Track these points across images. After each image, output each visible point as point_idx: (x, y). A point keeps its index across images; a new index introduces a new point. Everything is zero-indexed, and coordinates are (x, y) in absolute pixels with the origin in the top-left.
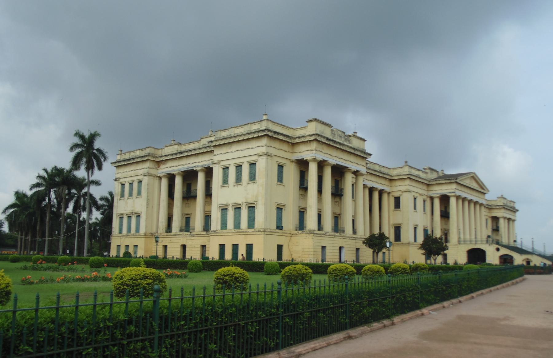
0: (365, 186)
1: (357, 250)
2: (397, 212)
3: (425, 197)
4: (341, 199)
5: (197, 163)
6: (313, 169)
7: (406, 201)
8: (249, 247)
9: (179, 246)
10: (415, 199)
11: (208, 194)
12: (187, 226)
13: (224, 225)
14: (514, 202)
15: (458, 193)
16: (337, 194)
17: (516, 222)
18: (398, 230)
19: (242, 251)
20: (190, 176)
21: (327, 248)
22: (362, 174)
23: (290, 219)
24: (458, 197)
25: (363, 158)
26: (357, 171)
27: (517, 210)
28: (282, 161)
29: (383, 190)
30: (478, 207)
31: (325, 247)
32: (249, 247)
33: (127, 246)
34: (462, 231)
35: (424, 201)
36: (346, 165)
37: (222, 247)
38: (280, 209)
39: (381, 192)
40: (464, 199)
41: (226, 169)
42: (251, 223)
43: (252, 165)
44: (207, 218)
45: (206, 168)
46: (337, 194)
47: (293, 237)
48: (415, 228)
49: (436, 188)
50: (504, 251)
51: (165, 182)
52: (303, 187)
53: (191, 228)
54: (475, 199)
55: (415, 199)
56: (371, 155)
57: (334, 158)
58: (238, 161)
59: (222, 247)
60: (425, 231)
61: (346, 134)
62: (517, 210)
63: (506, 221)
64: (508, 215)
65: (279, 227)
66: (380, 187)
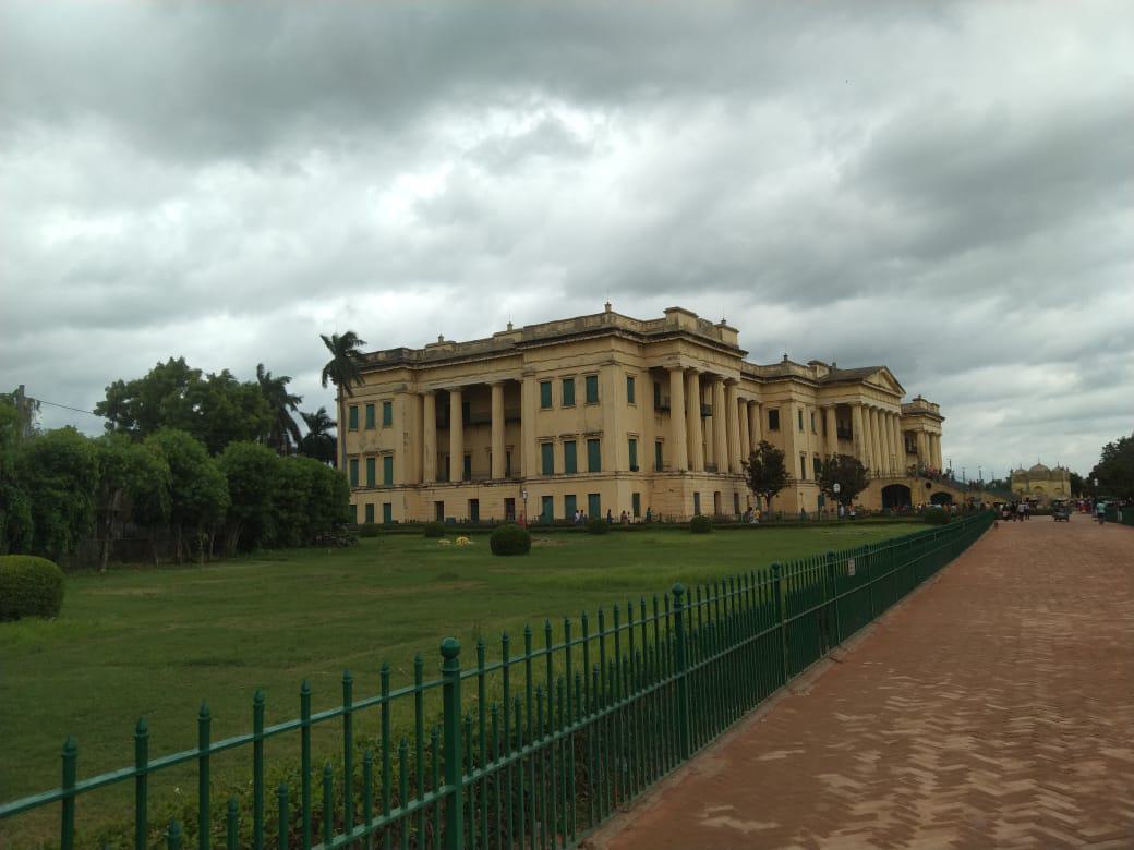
2: (775, 434)
3: (813, 408)
5: (491, 375)
7: (790, 416)
8: (594, 498)
9: (466, 502)
10: (800, 413)
11: (513, 420)
13: (548, 469)
14: (938, 406)
15: (864, 400)
16: (706, 412)
17: (941, 438)
19: (582, 504)
20: (475, 395)
21: (701, 495)
22: (736, 383)
23: (645, 458)
24: (864, 407)
25: (737, 359)
28: (632, 371)
30: (891, 418)
32: (594, 498)
36: (717, 372)
37: (547, 500)
38: (632, 443)
39: (750, 405)
40: (872, 409)
41: (546, 386)
42: (595, 464)
43: (592, 380)
44: (510, 453)
48: (803, 459)
49: (830, 393)
50: (938, 488)
51: (429, 404)
52: (662, 409)
54: (887, 407)
55: (800, 413)
56: (747, 353)
59: (547, 500)
60: (816, 461)
62: (943, 419)
63: (928, 437)
64: (929, 426)
65: (634, 468)
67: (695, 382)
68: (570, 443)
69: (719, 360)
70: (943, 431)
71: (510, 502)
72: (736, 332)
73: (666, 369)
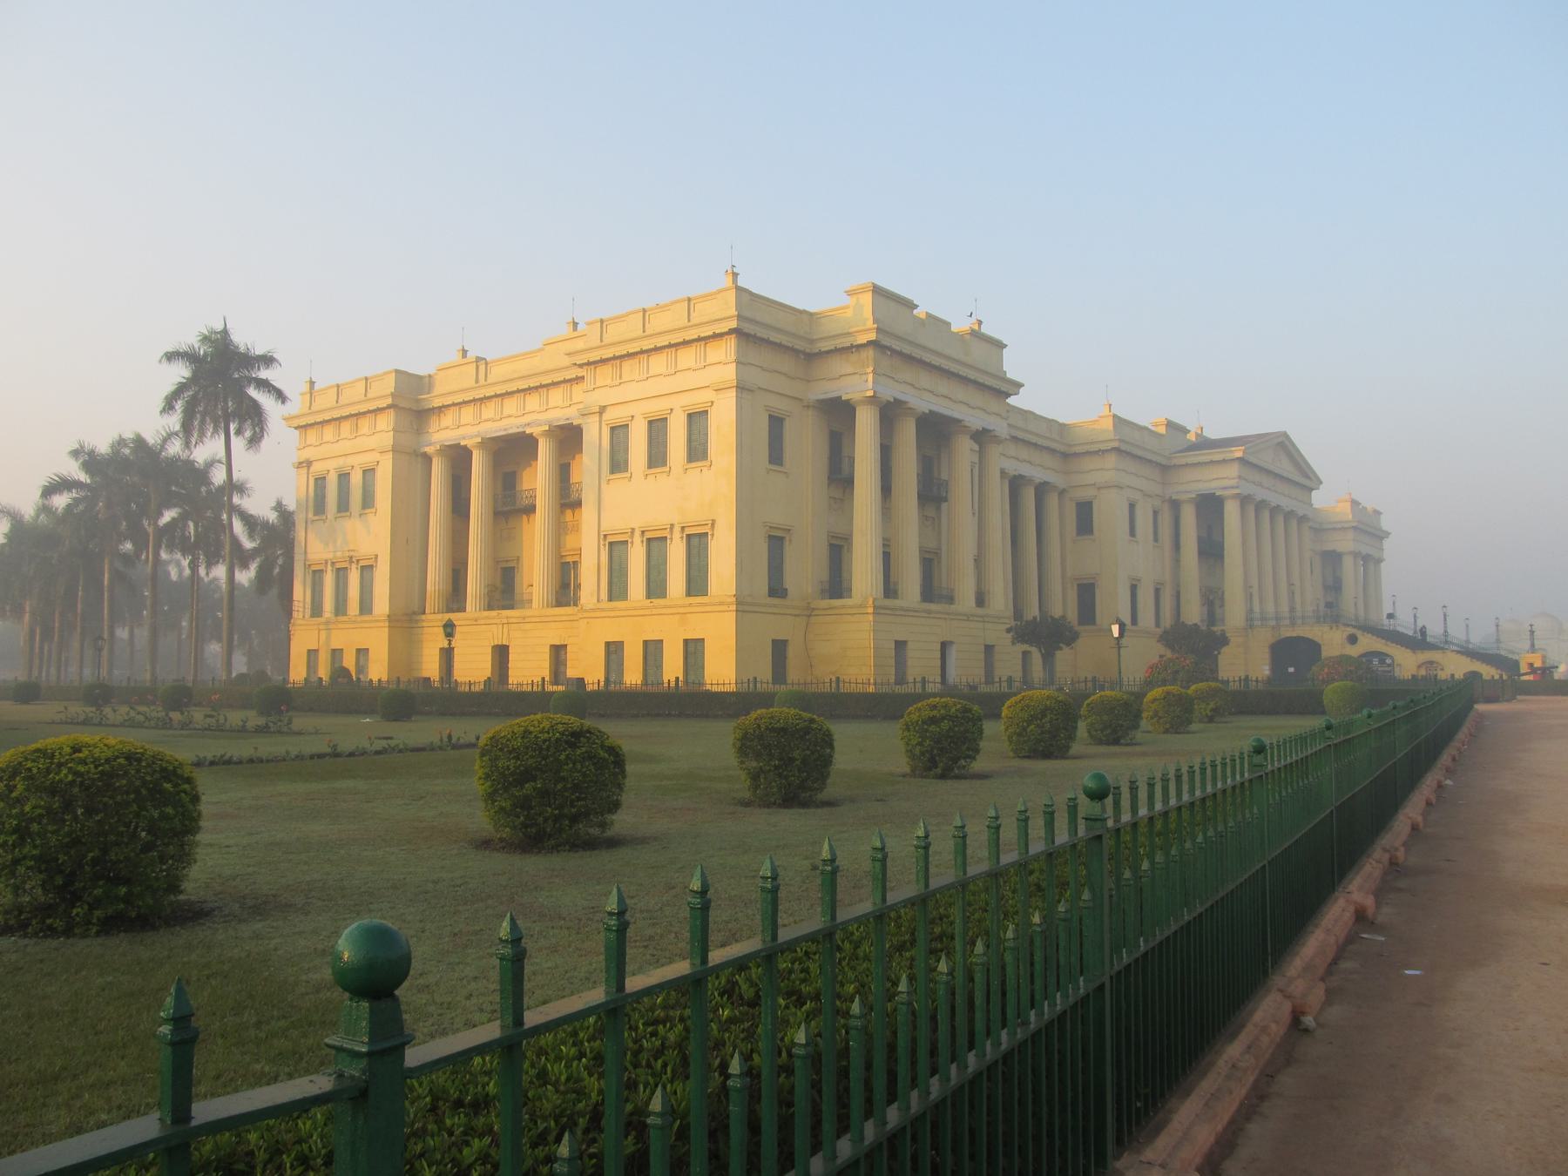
0: (1003, 473)
1: (989, 649)
4: (939, 509)
6: (866, 425)
11: (567, 501)
12: (504, 591)
16: (933, 494)
18: (1087, 593)
20: (511, 452)
21: (910, 645)
22: (997, 440)
23: (804, 570)
26: (985, 431)
27: (1387, 534)
29: (1046, 483)
31: (905, 643)
33: (336, 654)
34: (1255, 591)
35: (1155, 513)
36: (956, 415)
37: (614, 650)
38: (776, 543)
39: (1042, 490)
40: (1260, 506)
45: (561, 427)
46: (933, 494)
47: (813, 619)
48: (1134, 589)
50: (1367, 643)
52: (840, 477)
53: (517, 597)
54: (1286, 503)
55: (1132, 507)
56: (1019, 385)
57: (925, 396)
58: (656, 408)
61: (954, 329)
62: (1387, 534)
66: (1039, 475)
67: (907, 435)
68: (656, 544)
69: (960, 392)
70: (1386, 555)
71: (558, 651)
72: (1001, 346)
73: (848, 401)
